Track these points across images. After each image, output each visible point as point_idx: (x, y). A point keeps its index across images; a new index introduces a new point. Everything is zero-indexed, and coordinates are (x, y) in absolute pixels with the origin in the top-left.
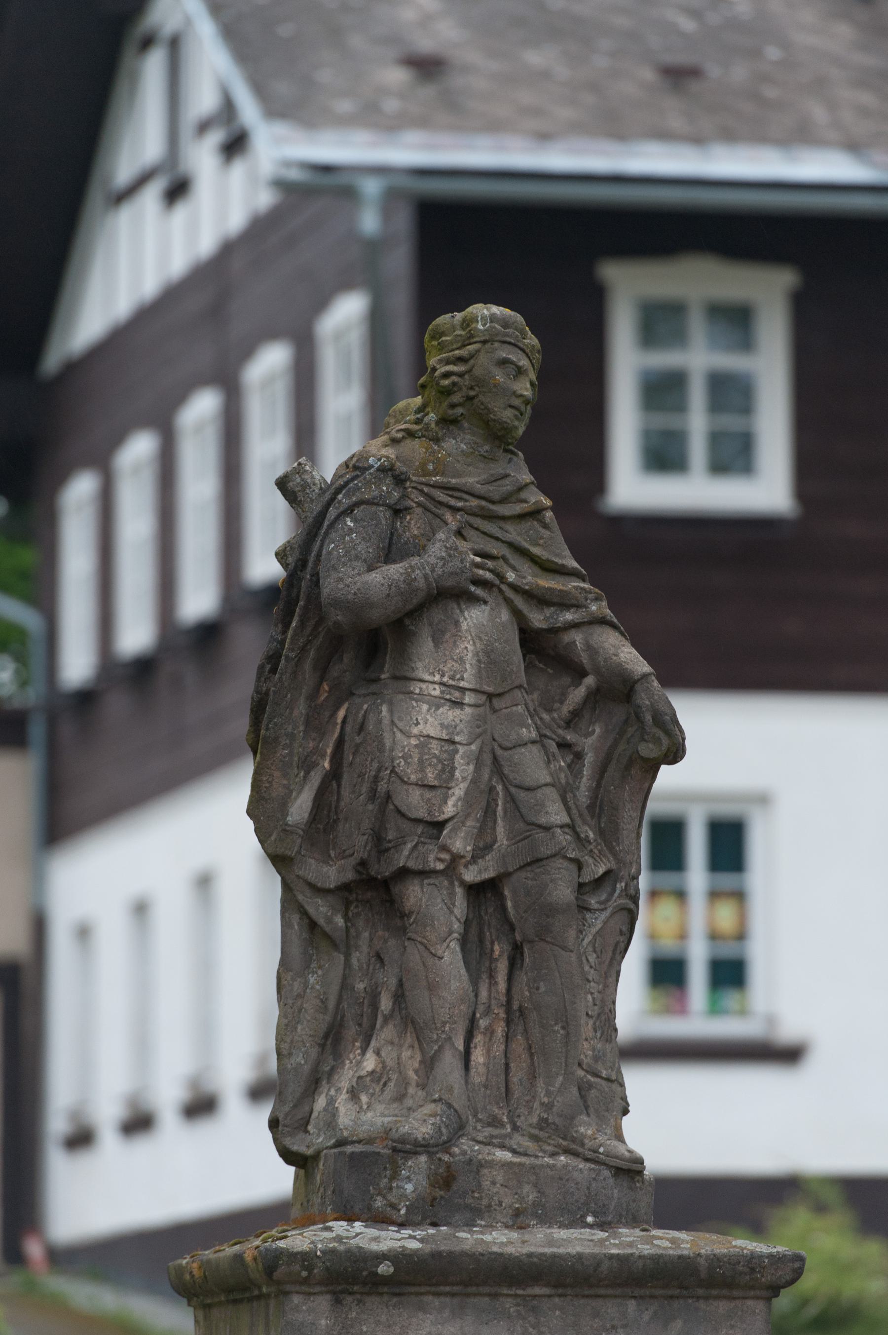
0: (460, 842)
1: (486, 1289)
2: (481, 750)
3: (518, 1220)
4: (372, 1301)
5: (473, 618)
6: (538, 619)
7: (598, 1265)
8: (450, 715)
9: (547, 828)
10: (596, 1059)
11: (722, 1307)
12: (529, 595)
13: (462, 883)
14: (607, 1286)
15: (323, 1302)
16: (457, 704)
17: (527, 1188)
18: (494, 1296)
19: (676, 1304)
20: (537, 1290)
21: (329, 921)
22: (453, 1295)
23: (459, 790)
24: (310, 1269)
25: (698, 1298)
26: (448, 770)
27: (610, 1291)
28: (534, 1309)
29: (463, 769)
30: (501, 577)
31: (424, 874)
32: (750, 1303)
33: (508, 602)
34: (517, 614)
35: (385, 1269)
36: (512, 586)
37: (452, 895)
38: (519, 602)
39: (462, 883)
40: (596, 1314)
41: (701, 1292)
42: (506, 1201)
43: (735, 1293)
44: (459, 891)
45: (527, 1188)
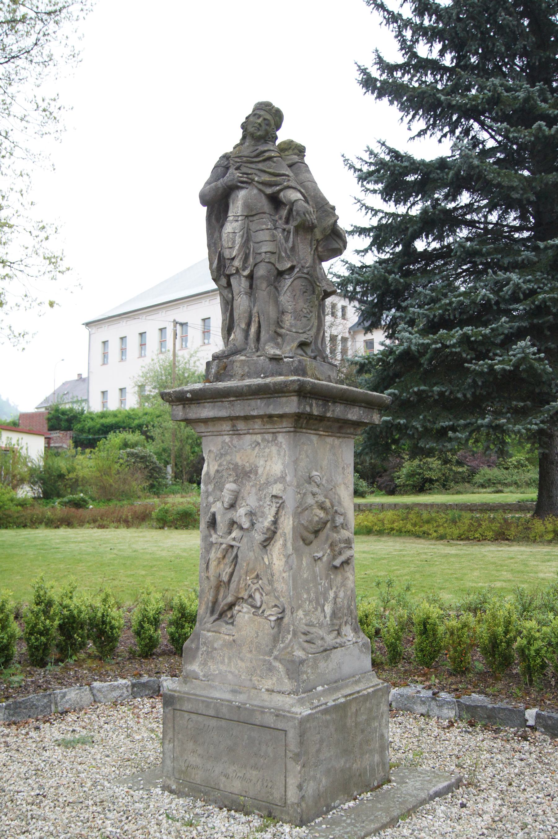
0: (237, 263)
1: (219, 400)
2: (243, 234)
3: (243, 377)
4: (192, 406)
5: (242, 194)
6: (269, 191)
7: (243, 388)
8: (235, 224)
9: (260, 254)
10: (291, 326)
11: (284, 399)
12: (263, 183)
13: (244, 276)
14: (250, 395)
15: (181, 407)
16: (237, 221)
17: (246, 367)
18: (222, 402)
19: (272, 400)
20: (232, 399)
21: (227, 296)
22: (212, 402)
23: (237, 248)
24: (171, 397)
25: (277, 397)
26: (234, 242)
27: (251, 397)
28: (233, 405)
29: (238, 240)
30: (253, 180)
31: (232, 275)
32: (292, 398)
33: (256, 187)
34: (260, 190)
35: (189, 395)
36: (257, 182)
37: (240, 280)
38: (260, 186)
39: (244, 276)
40: (249, 406)
41: (276, 395)
42: (240, 372)
43: (286, 394)
44: (243, 279)
45: (246, 367)
